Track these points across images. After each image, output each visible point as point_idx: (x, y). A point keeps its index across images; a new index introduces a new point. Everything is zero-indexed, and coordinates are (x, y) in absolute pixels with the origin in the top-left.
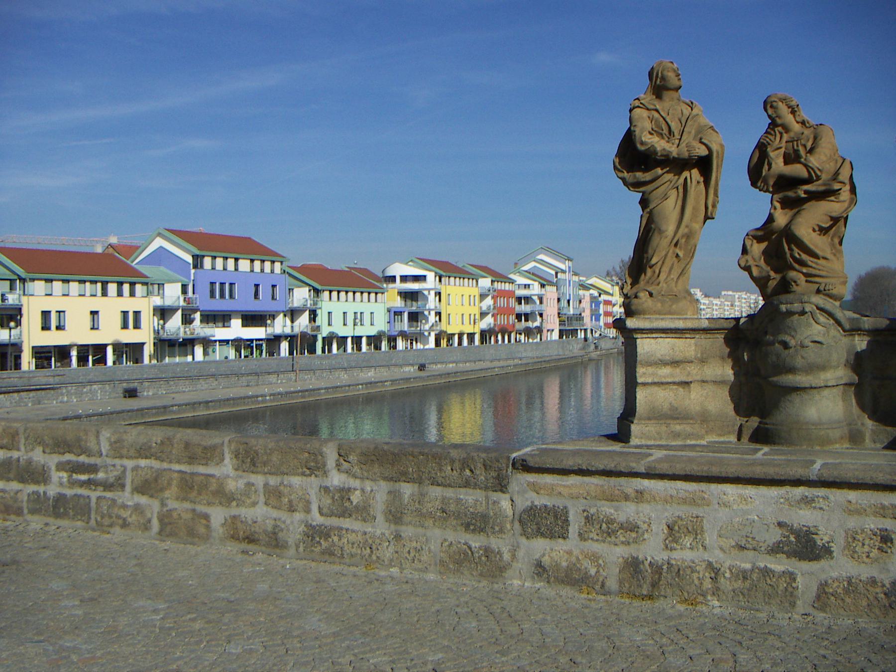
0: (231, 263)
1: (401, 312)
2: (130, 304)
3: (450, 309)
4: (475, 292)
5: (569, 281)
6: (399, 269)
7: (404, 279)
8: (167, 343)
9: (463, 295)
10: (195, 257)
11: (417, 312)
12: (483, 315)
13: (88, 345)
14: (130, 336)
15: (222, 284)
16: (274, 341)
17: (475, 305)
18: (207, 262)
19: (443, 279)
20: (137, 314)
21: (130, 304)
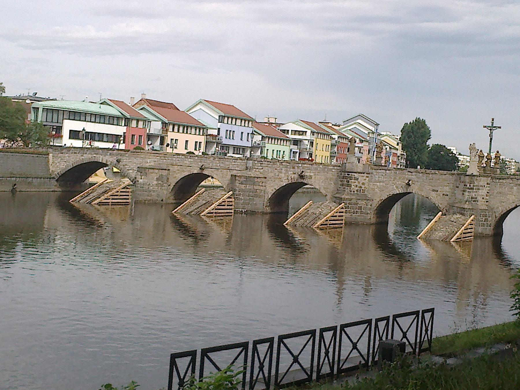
4: (329, 143)
5: (376, 139)
6: (290, 127)
9: (323, 145)
17: (328, 151)
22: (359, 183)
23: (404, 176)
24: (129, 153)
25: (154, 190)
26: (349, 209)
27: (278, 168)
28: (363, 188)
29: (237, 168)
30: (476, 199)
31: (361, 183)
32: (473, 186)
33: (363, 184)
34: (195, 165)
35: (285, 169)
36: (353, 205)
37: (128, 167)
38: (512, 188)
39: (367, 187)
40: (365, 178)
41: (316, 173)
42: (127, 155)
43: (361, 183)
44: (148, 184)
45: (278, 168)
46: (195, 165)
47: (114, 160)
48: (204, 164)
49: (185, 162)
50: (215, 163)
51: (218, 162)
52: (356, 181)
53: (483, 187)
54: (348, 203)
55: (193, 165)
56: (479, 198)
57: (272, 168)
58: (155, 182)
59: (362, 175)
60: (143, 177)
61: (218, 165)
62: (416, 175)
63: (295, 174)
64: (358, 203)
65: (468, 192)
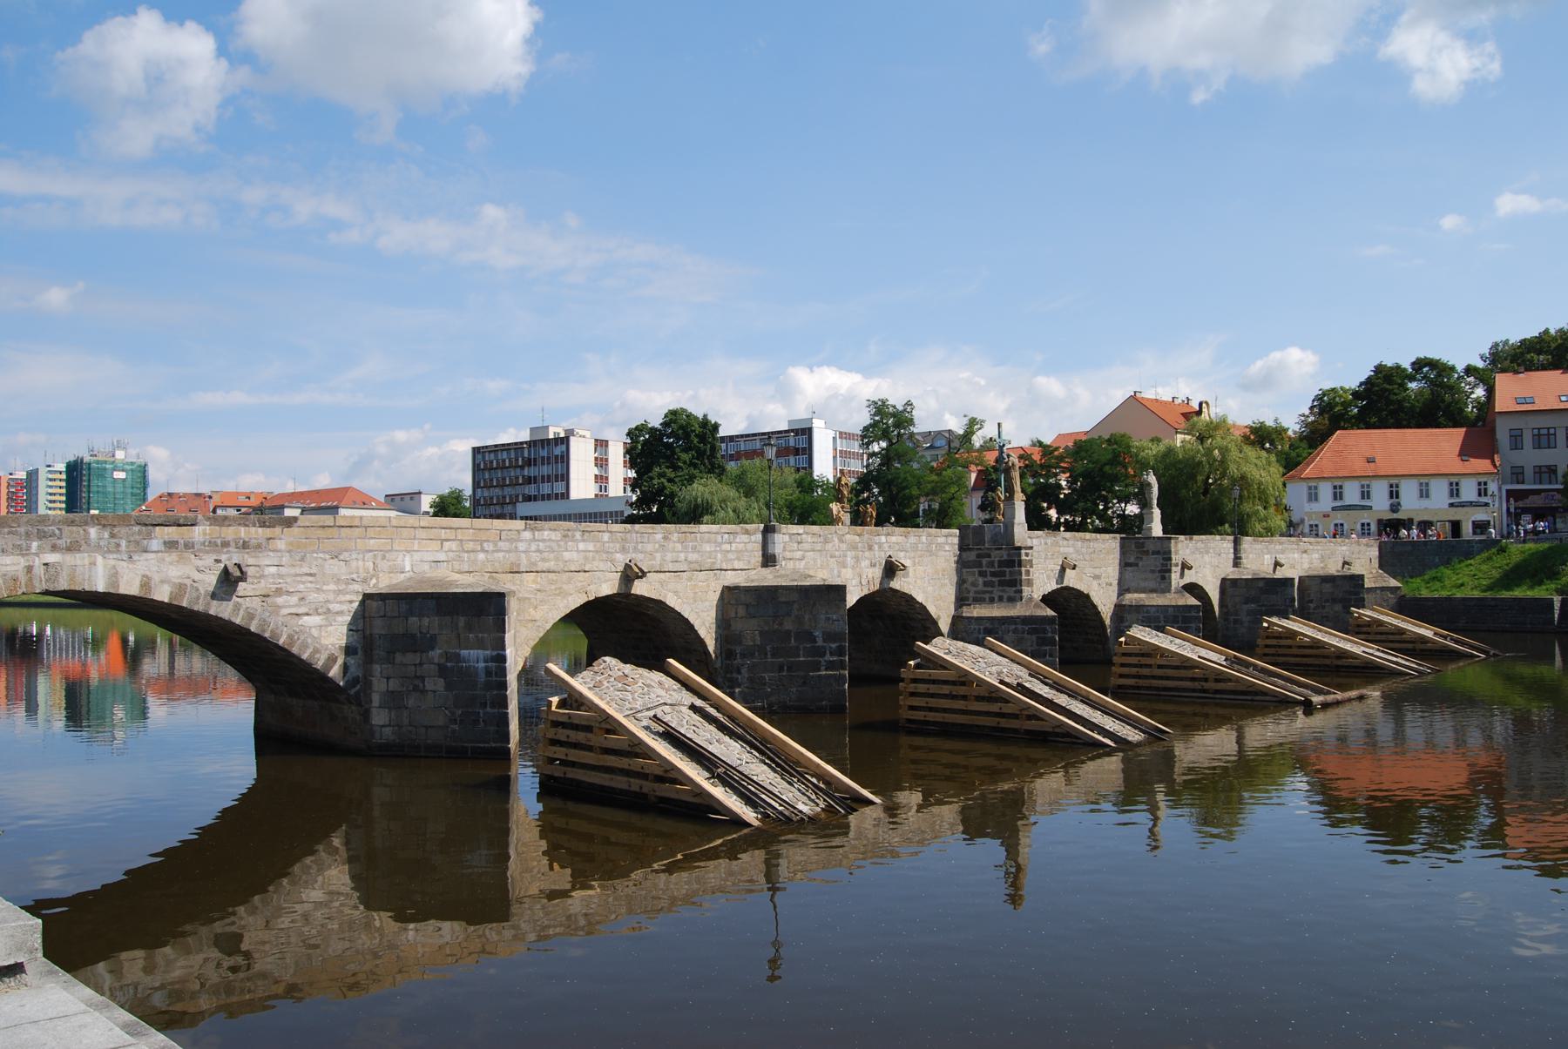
23: (1058, 548)
24: (295, 530)
27: (837, 553)
29: (736, 562)
34: (602, 566)
35: (853, 553)
37: (294, 599)
41: (917, 561)
42: (281, 545)
45: (837, 553)
46: (602, 566)
47: (197, 576)
48: (634, 555)
49: (567, 555)
50: (672, 552)
51: (679, 546)
55: (596, 563)
57: (825, 552)
61: (682, 556)
62: (1073, 546)
63: (874, 565)
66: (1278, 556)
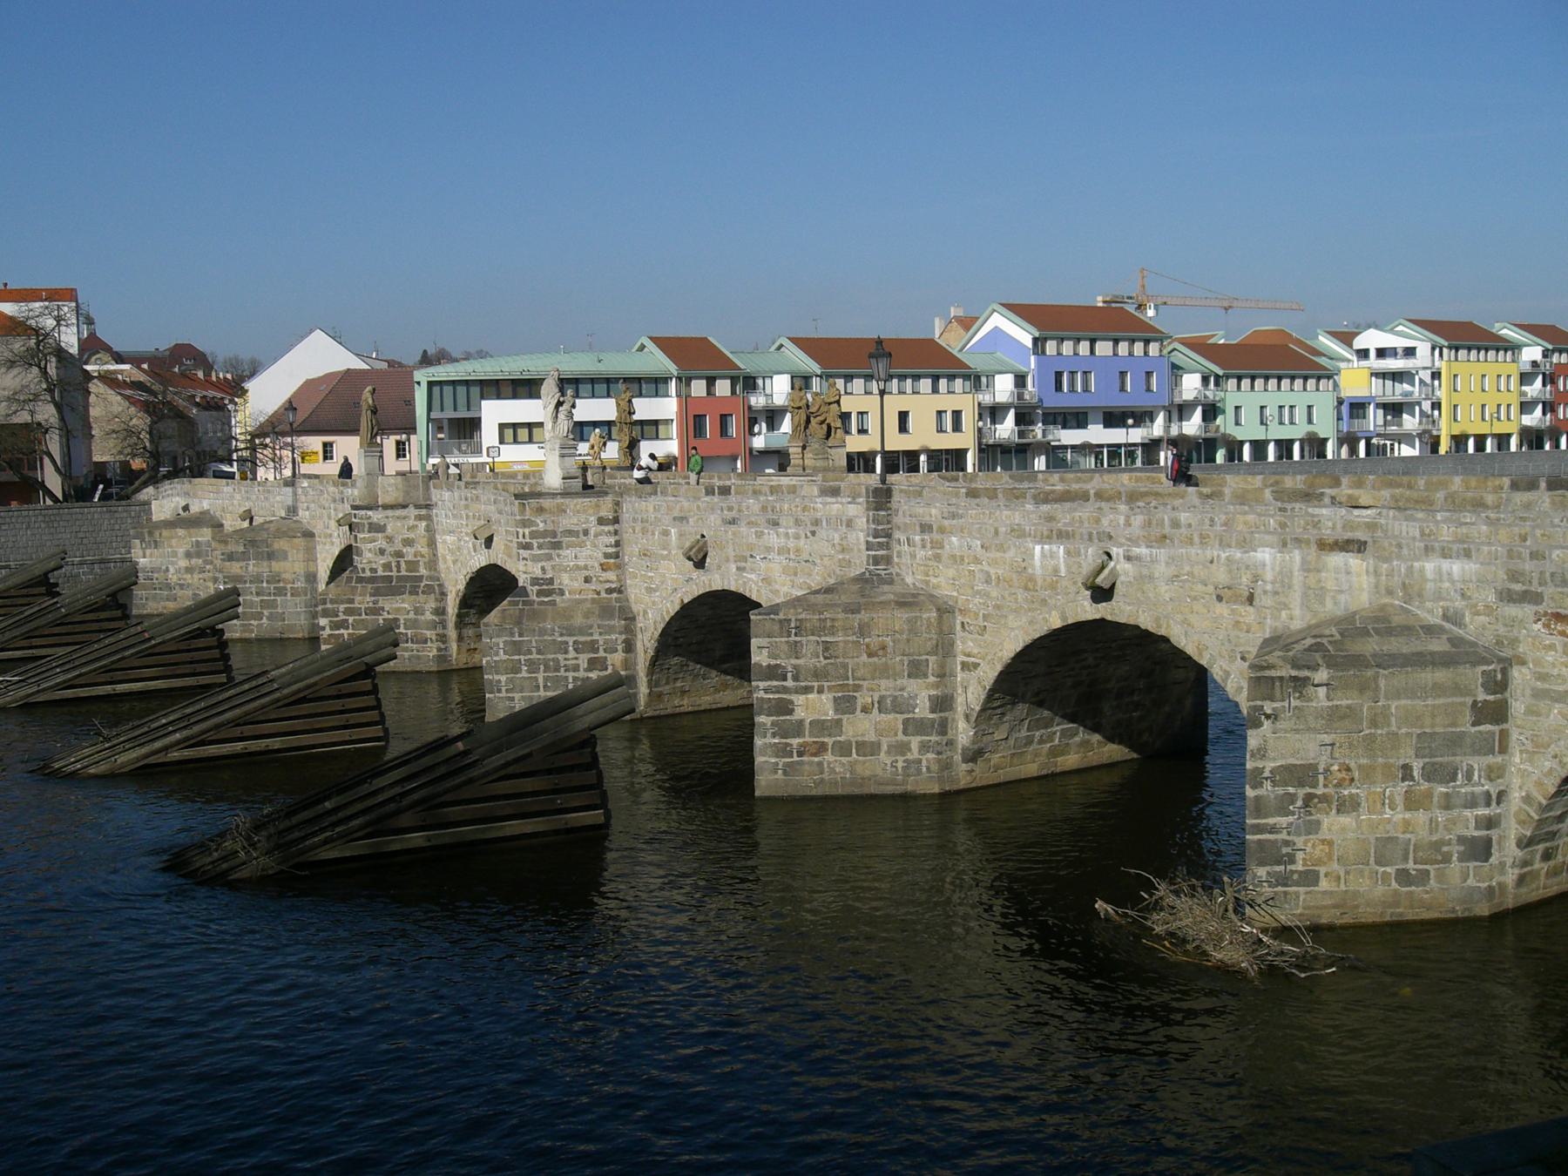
0: (1084, 348)
1: (1364, 404)
2: (948, 403)
3: (1456, 398)
7: (1381, 353)
8: (999, 449)
10: (1035, 340)
11: (1401, 404)
12: (1525, 407)
13: (898, 452)
14: (949, 441)
15: (1073, 373)
16: (1151, 447)
18: (1051, 347)
19: (1445, 351)
20: (957, 415)
21: (948, 403)
22: (390, 539)
25: (182, 582)
26: (351, 631)
28: (410, 558)
30: (553, 584)
31: (399, 538)
32: (533, 535)
33: (408, 542)
36: (364, 617)
38: (666, 533)
39: (425, 550)
40: (411, 522)
43: (399, 538)
44: (164, 568)
52: (380, 535)
53: (581, 535)
54: (341, 610)
56: (566, 581)
58: (183, 563)
59: (399, 512)
60: (148, 552)
64: (383, 609)
65: (524, 559)
66: (1114, 551)
